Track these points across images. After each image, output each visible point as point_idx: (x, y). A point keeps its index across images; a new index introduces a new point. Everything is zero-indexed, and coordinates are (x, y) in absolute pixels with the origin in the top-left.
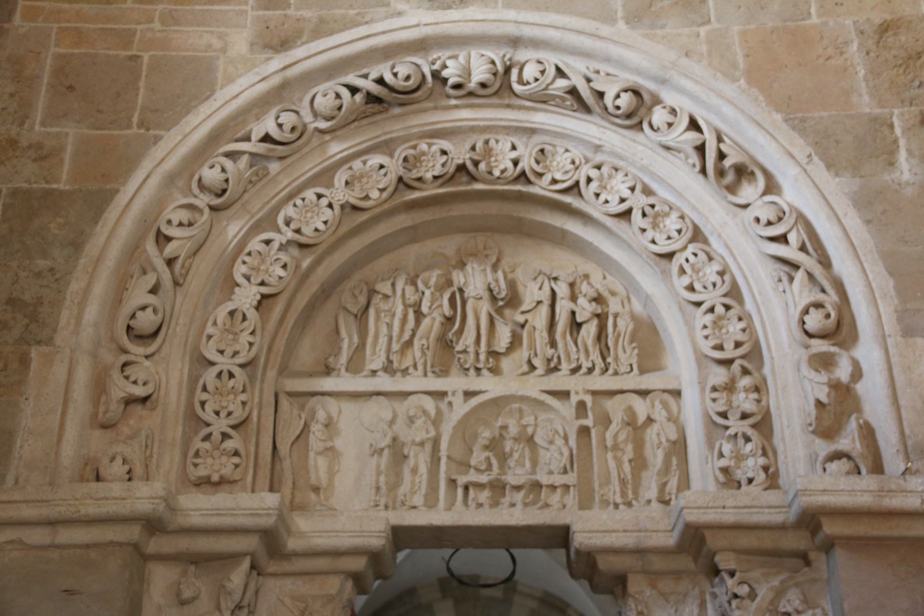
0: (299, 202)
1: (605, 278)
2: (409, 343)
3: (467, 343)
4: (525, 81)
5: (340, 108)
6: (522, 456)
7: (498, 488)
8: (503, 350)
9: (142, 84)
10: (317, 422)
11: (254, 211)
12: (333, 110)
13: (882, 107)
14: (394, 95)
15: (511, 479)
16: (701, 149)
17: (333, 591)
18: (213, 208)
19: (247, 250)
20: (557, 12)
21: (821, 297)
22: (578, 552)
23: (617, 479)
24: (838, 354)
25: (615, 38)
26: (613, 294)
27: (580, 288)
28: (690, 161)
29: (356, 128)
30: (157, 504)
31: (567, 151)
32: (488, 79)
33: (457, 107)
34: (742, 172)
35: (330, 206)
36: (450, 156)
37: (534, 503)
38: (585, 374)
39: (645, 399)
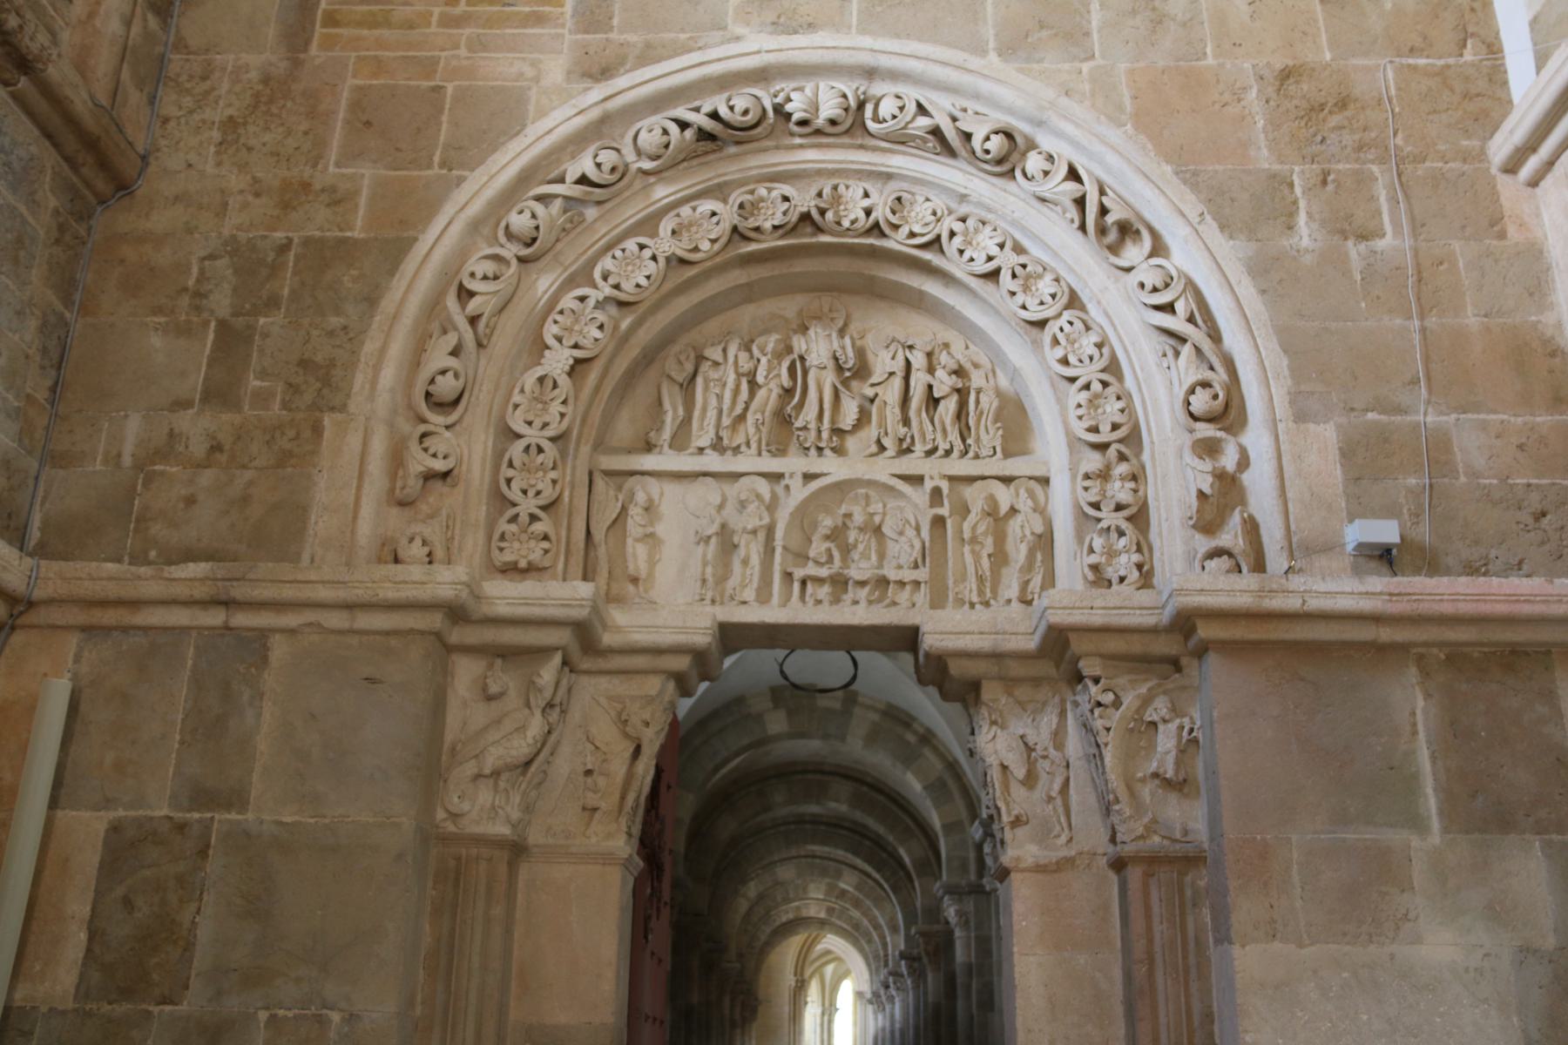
0: (618, 253)
1: (967, 347)
2: (742, 418)
3: (808, 419)
4: (881, 119)
5: (667, 146)
6: (868, 547)
7: (840, 583)
8: (848, 428)
9: (445, 118)
10: (636, 505)
11: (567, 263)
12: (659, 148)
13: (1282, 163)
14: (730, 131)
15: (855, 573)
16: (1080, 202)
17: (653, 693)
18: (522, 260)
19: (559, 308)
20: (920, 40)
21: (1209, 375)
22: (927, 655)
23: (974, 576)
24: (1225, 440)
25: (986, 72)
26: (976, 366)
27: (938, 359)
28: (1069, 215)
29: (686, 169)
30: (460, 591)
31: (928, 200)
32: (839, 115)
33: (801, 146)
34: (1126, 230)
35: (654, 258)
36: (793, 202)
37: (879, 600)
38: (941, 457)
39: (1008, 486)
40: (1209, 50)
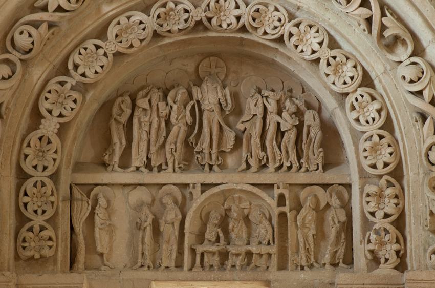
2: (163, 146)
3: (203, 146)
16: (369, 21)
23: (303, 249)
35: (105, 55)
38: (285, 171)
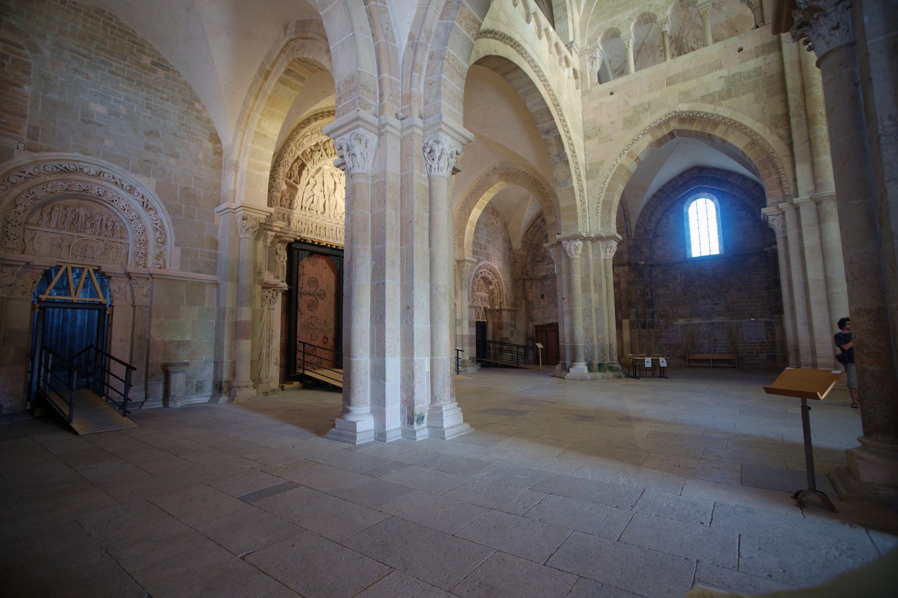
16: (144, 202)
34: (150, 209)
40: (172, 180)
